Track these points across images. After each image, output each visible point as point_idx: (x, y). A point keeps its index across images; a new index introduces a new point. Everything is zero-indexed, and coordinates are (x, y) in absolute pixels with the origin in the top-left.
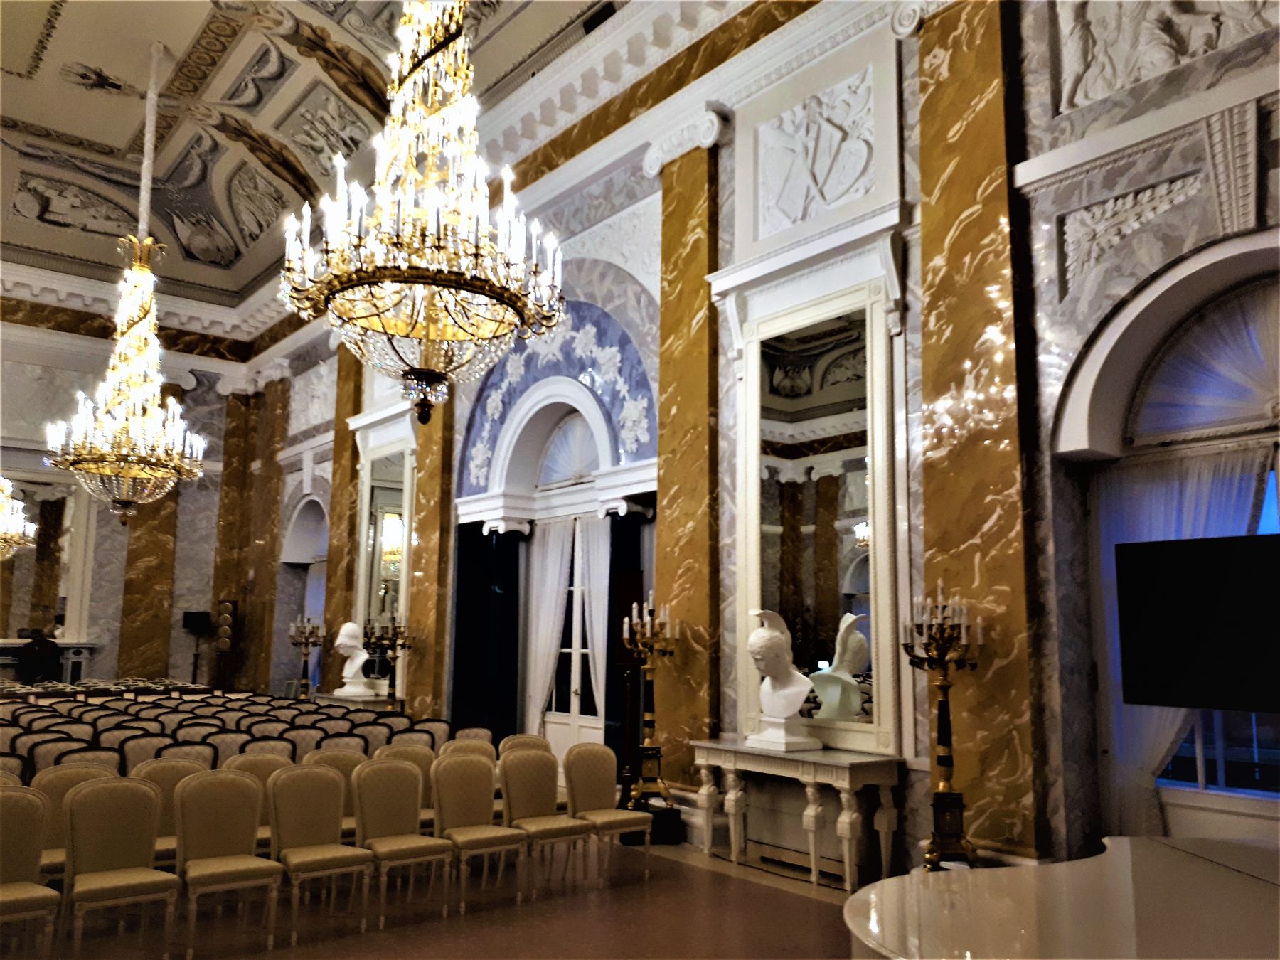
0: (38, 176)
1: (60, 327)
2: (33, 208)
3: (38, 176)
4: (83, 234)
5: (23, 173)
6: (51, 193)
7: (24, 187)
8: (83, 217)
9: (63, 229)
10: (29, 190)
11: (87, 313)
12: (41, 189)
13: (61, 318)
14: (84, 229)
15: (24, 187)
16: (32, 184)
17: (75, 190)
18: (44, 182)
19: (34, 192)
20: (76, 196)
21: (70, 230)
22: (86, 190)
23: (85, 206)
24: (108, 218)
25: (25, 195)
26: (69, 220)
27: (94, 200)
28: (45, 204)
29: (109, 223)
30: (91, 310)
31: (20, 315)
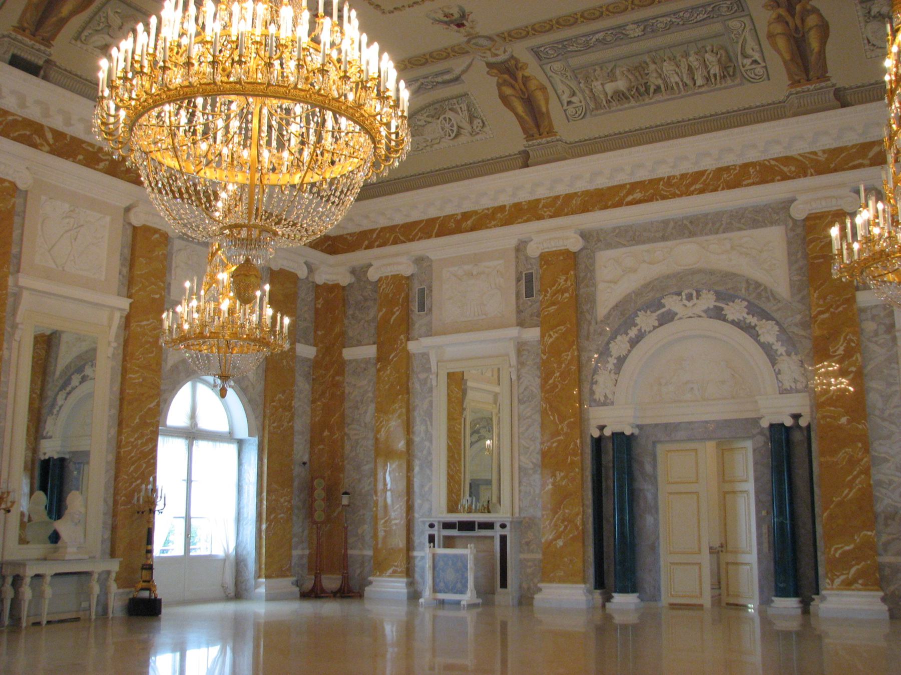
10: (874, 17)
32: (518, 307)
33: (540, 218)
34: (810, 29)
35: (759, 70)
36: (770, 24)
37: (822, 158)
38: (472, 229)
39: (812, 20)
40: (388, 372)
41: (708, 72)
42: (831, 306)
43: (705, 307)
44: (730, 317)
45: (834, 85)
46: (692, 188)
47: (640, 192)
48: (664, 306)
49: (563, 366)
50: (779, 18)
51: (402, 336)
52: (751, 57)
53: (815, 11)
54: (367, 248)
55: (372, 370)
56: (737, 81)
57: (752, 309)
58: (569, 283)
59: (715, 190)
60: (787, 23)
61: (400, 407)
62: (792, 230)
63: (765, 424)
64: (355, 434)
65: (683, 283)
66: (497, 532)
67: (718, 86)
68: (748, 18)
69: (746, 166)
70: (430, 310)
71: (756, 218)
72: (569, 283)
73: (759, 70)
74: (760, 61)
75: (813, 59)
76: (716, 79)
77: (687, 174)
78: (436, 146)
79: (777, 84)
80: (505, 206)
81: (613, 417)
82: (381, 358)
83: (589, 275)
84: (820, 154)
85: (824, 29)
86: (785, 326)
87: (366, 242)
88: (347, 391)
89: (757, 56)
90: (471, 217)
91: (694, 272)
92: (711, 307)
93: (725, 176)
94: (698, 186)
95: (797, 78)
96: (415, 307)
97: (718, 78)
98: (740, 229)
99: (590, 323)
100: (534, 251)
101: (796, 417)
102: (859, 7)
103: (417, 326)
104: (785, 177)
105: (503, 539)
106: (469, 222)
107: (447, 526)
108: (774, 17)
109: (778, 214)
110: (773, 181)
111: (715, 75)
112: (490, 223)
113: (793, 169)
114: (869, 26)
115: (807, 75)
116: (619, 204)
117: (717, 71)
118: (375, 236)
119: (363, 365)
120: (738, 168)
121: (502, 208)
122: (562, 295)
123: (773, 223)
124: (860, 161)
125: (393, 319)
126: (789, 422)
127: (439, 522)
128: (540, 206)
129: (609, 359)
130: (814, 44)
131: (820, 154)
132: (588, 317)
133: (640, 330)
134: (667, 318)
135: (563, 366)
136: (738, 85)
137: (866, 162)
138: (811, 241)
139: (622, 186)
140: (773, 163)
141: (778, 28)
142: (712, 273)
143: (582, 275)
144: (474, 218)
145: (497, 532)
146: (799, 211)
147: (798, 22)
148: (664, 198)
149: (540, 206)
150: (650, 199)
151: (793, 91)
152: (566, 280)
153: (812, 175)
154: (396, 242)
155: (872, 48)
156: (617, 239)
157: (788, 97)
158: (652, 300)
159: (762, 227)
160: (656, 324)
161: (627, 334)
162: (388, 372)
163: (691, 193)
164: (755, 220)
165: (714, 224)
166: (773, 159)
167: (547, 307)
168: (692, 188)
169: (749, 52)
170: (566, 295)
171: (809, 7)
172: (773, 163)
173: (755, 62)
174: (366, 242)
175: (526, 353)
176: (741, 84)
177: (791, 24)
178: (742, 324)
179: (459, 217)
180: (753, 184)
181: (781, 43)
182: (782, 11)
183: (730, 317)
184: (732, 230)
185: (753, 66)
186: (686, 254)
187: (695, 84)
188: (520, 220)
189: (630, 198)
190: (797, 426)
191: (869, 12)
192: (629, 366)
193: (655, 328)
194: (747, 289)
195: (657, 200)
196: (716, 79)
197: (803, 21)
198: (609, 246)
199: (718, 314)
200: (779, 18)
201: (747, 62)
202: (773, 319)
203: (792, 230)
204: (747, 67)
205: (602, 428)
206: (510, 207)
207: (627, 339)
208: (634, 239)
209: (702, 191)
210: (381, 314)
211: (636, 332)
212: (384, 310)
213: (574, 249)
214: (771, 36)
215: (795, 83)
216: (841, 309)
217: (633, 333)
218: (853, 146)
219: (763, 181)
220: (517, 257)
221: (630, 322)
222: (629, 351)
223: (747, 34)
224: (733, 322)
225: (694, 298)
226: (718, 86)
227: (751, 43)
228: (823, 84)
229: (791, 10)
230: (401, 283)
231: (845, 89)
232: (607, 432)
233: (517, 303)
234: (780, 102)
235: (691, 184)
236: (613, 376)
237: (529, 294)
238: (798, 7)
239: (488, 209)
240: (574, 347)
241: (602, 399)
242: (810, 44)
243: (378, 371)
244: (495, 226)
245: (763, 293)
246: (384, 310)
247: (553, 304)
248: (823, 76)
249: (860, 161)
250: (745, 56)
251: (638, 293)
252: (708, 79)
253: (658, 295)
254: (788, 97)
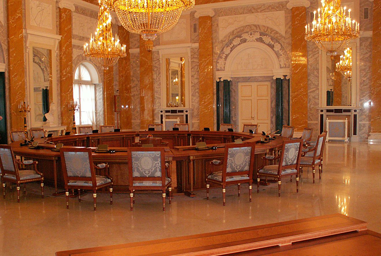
63: (274, 78)
66: (185, 114)
81: (224, 75)
100: (197, 15)
101: (285, 76)
105: (187, 116)
107: (167, 112)
126: (282, 78)
127: (164, 110)
129: (224, 55)
134: (245, 41)
145: (185, 114)
158: (238, 35)
190: (285, 79)
199: (260, 40)
205: (220, 78)
213: (211, 16)
225: (253, 34)
232: (222, 80)
236: (224, 61)
237: (195, 31)
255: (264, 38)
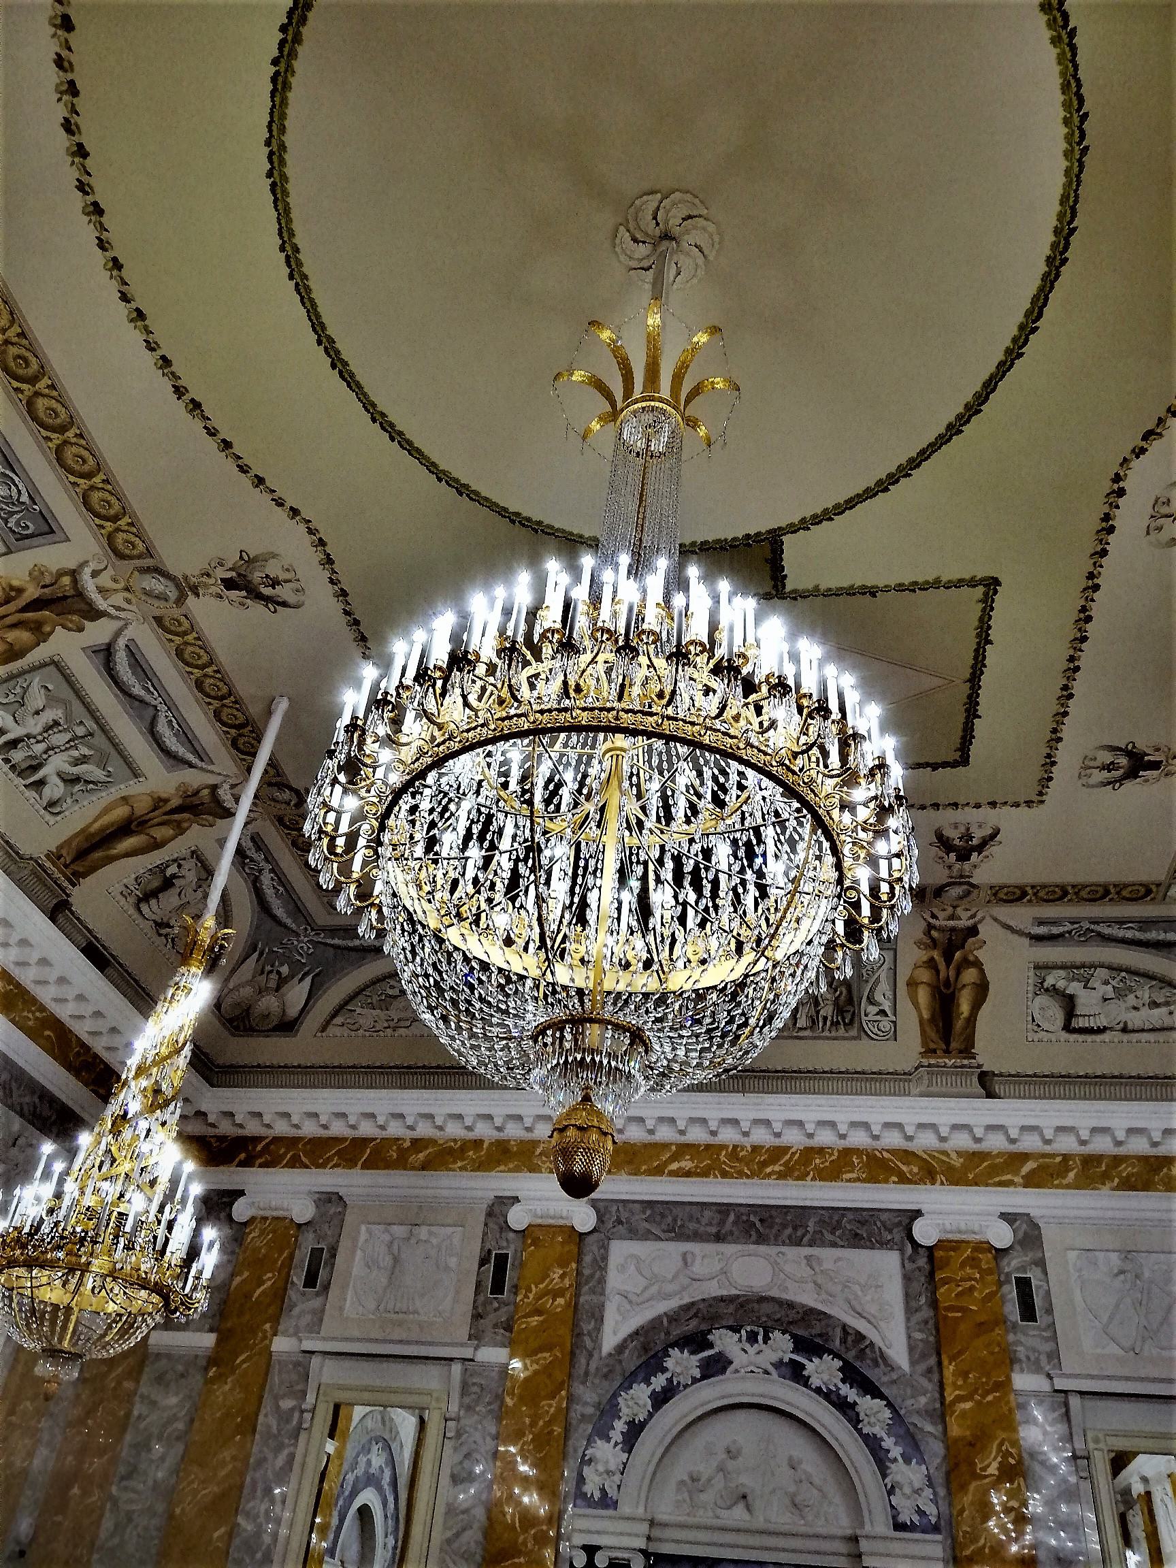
0: (1056, 967)
1: (1128, 1185)
2: (1056, 1014)
3: (1056, 967)
4: (1125, 1037)
5: (1037, 967)
6: (1074, 988)
7: (1041, 988)
8: (1119, 1012)
9: (1098, 1038)
10: (1047, 990)
11: (1157, 1157)
12: (1061, 984)
13: (1125, 1170)
14: (1125, 1030)
15: (1041, 988)
16: (1050, 981)
17: (1102, 973)
18: (1062, 973)
19: (1054, 991)
20: (1106, 983)
21: (1106, 1037)
22: (1119, 969)
23: (1120, 994)
24: (1154, 1004)
25: (1043, 1000)
26: (1102, 1022)
27: (1131, 981)
28: (1069, 1004)
29: (1156, 1011)
30: (1161, 1151)
31: (1072, 1175)
32: (475, 1308)
33: (534, 1169)
34: (964, 986)
35: (885, 1024)
36: (916, 967)
37: (957, 1162)
38: (424, 1167)
39: (970, 975)
40: (227, 1387)
41: (818, 1012)
42: (976, 1390)
43: (775, 1357)
44: (815, 1382)
45: (979, 1066)
46: (768, 1170)
47: (692, 1160)
48: (711, 1346)
49: (541, 1423)
50: (931, 964)
51: (267, 1326)
52: (880, 1005)
53: (977, 964)
54: (242, 1164)
55: (197, 1380)
56: (854, 1032)
57: (850, 1374)
58: (567, 1282)
59: (802, 1177)
60: (938, 972)
61: (234, 1458)
62: (912, 1259)
64: (132, 1501)
65: (752, 1314)
67: (826, 1033)
68: (892, 952)
69: (847, 1152)
70: (326, 1287)
71: (860, 1229)
72: (567, 1282)
73: (885, 1024)
74: (889, 1013)
75: (959, 1024)
76: (825, 1023)
77: (763, 1147)
78: (402, 1031)
79: (908, 1047)
80: (482, 1141)
82: (217, 1360)
83: (598, 1274)
84: (954, 1155)
85: (982, 989)
86: (902, 1412)
87: (243, 1156)
88: (136, 1413)
89: (887, 1006)
90: (426, 1148)
91: (763, 1299)
92: (786, 1360)
93: (818, 1161)
94: (777, 1168)
95: (932, 1046)
96: (298, 1278)
97: (828, 1023)
98: (834, 1245)
99: (591, 1355)
100: (518, 1218)
102: (1031, 973)
103: (296, 1311)
104: (903, 1179)
106: (421, 1156)
108: (925, 958)
109: (890, 1231)
110: (886, 1181)
111: (825, 1018)
112: (455, 1162)
113: (915, 1170)
114: (1038, 999)
115: (948, 1043)
116: (658, 1171)
117: (830, 1013)
118: (259, 1148)
119: (180, 1368)
120: (836, 1154)
121: (478, 1143)
122: (554, 1300)
123: (884, 1245)
124: (1009, 1177)
125: (258, 1292)
128: (538, 1151)
130: (965, 1008)
131: (954, 1155)
132: (588, 1342)
133: (670, 1380)
134: (716, 1366)
135: (541, 1423)
136: (854, 1038)
137: (1017, 1179)
138: (945, 1281)
139: (665, 1146)
140: (886, 1155)
141: (925, 975)
142: (791, 1305)
143: (587, 1272)
144: (430, 1150)
146: (925, 1233)
147: (952, 973)
148: (725, 1174)
149: (538, 1151)
150: (705, 1173)
151: (925, 1062)
152: (562, 1277)
153: (942, 1183)
154: (295, 1163)
155: (1036, 1028)
156: (647, 1225)
157: (916, 1069)
159: (866, 1248)
160: (697, 1373)
161: (649, 1384)
162: (227, 1387)
163: (769, 1175)
164: (857, 1235)
165: (795, 1228)
166: (888, 1151)
167: (525, 1316)
168: (768, 1170)
169: (878, 997)
170: (560, 1301)
171: (971, 958)
172: (886, 1155)
173: (883, 1013)
174: (243, 1156)
175: (475, 1389)
176: (858, 1038)
177: (942, 975)
178: (834, 1397)
179: (407, 1144)
180: (858, 1180)
181: (923, 995)
182: (936, 954)
183: (815, 1382)
184: (823, 1244)
185: (878, 1018)
186: (749, 1269)
187: (795, 1024)
188: (502, 1168)
189: (674, 1166)
191: (1042, 983)
192: (649, 1443)
193: (695, 1380)
194: (844, 1341)
195: (716, 1177)
196: (825, 1023)
197: (958, 974)
198: (634, 1234)
199: (795, 1373)
200: (931, 964)
201: (873, 1010)
202: (882, 1396)
203: (912, 1259)
204: (870, 1017)
206: (491, 1144)
207: (649, 1391)
208: (672, 1230)
209: (781, 1176)
210: (238, 1279)
211: (664, 1383)
212: (246, 1274)
214: (912, 984)
215: (929, 1052)
216: (990, 1398)
217: (659, 1382)
218: (1000, 1154)
219: (872, 1179)
220: (486, 1225)
221: (652, 1364)
222: (651, 1415)
223: (883, 974)
224: (818, 1391)
226: (826, 1033)
227: (884, 987)
228: (966, 1062)
229: (948, 957)
230: (284, 1230)
231: (994, 1075)
233: (475, 1302)
234: (905, 1074)
235: (764, 1164)
237: (498, 1287)
238: (958, 955)
239: (455, 1141)
240: (563, 1393)
241: (597, 1495)
242: (958, 1005)
243: (209, 1382)
244: (461, 1169)
245: (868, 1351)
246: (246, 1274)
247: (539, 1312)
248: (967, 1050)
249: (1009, 1177)
250: (871, 1001)
251: (674, 1317)
252: (814, 1022)
253: (704, 1327)
254: (916, 1069)
255: (812, 1367)
